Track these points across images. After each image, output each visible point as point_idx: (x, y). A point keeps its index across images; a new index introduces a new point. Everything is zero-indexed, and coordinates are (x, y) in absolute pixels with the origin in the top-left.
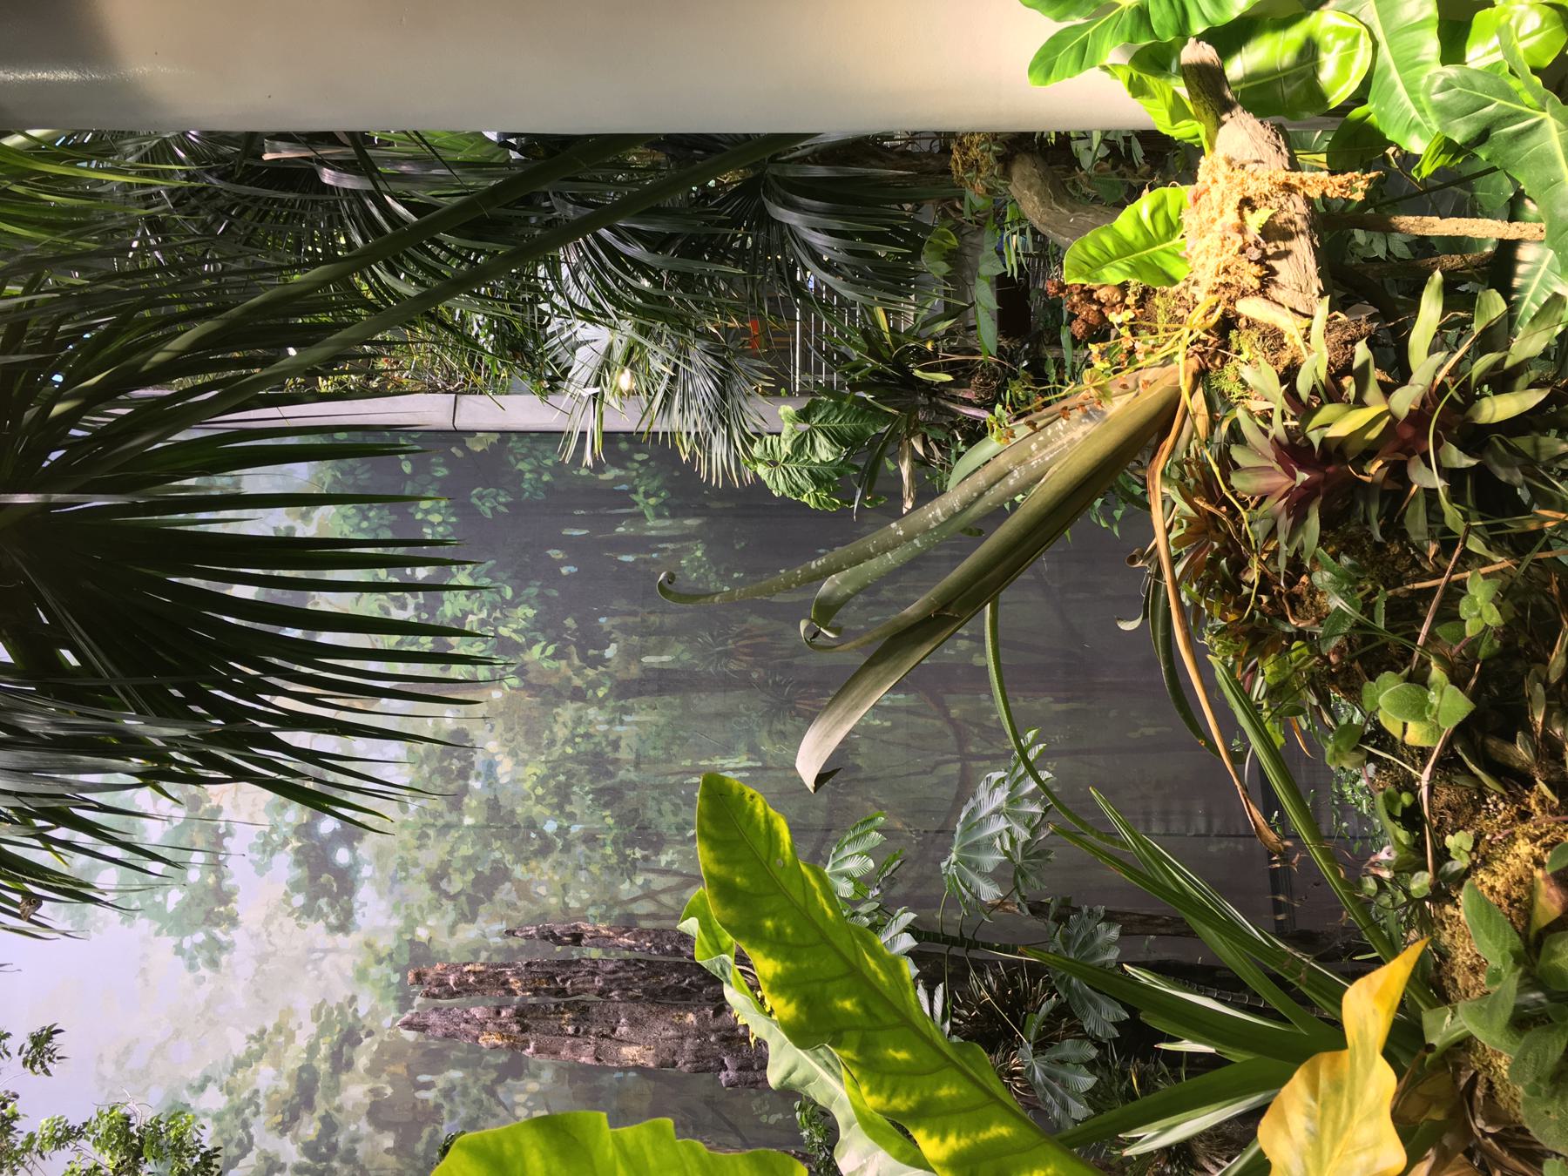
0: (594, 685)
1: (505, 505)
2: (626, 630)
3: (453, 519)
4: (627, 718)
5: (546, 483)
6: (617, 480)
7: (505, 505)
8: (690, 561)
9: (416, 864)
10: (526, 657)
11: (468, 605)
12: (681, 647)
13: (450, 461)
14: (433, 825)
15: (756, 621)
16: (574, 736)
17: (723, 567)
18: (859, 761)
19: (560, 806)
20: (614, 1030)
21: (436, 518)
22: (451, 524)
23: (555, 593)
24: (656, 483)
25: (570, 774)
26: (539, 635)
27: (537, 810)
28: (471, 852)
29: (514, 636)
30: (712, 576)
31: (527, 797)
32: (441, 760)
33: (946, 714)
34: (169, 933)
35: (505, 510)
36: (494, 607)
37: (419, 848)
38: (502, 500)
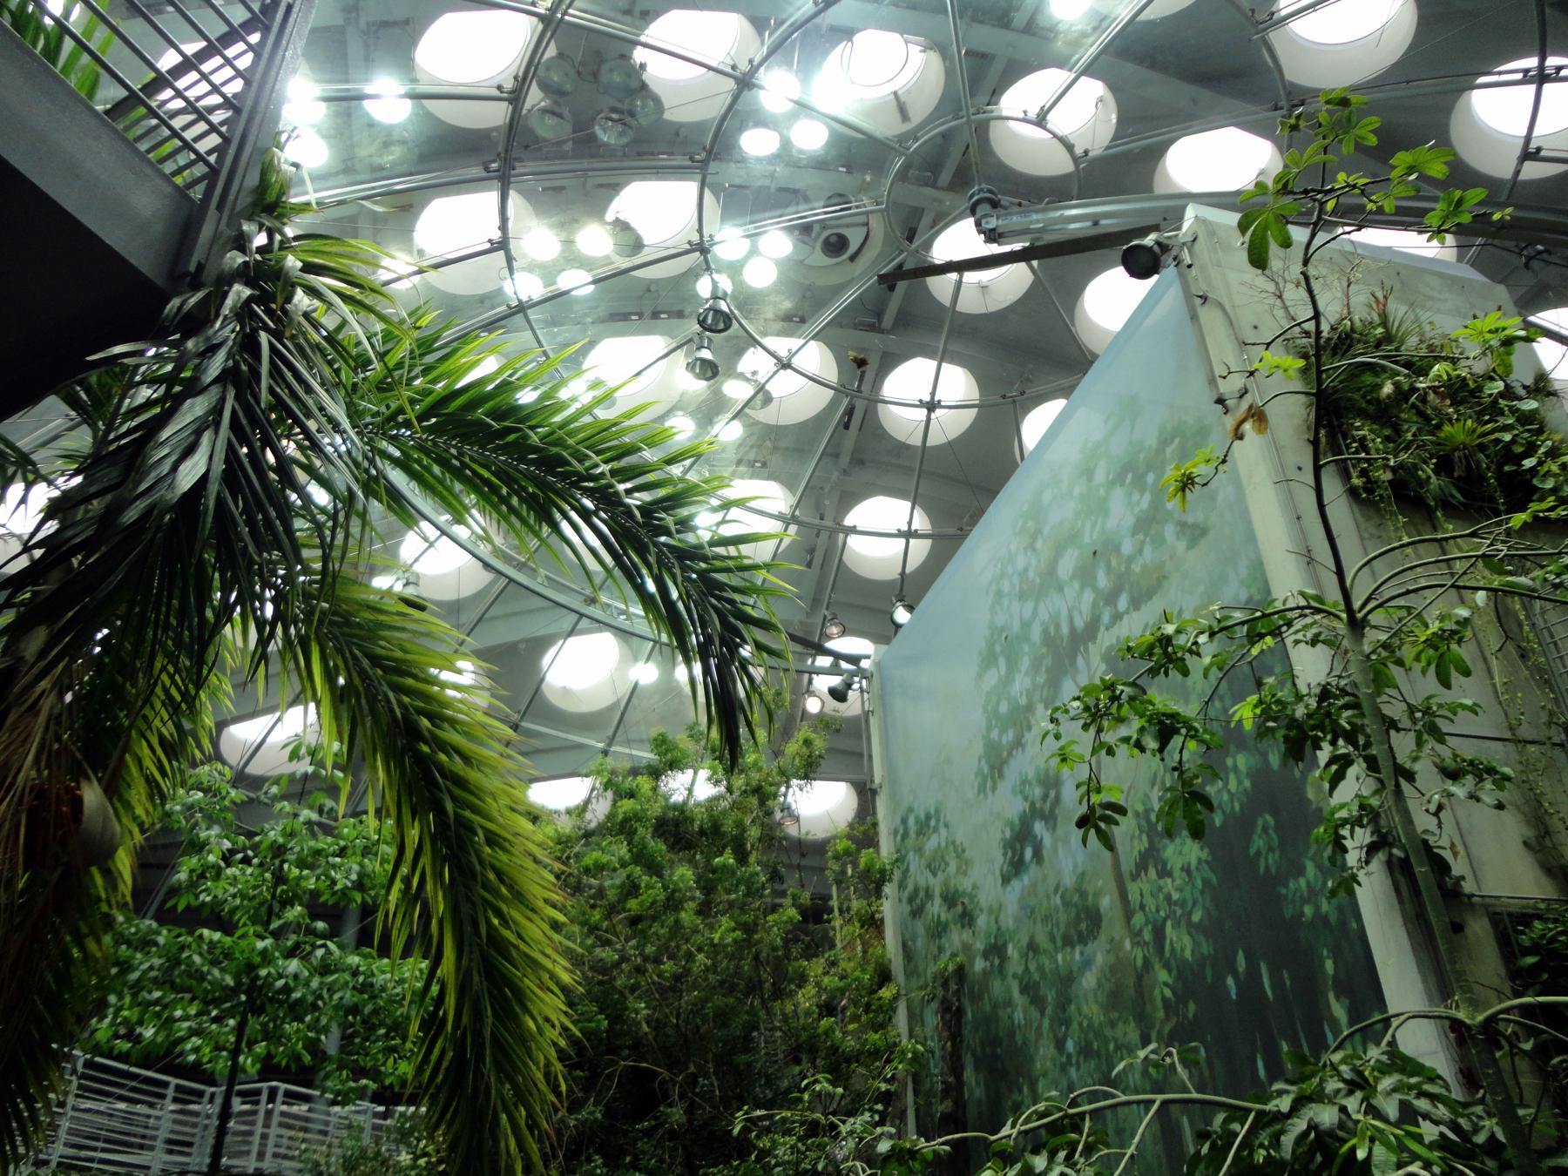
1: (1267, 867)
3: (1237, 806)
10: (1157, 966)
27: (1075, 1026)
31: (1079, 1010)
35: (1262, 870)
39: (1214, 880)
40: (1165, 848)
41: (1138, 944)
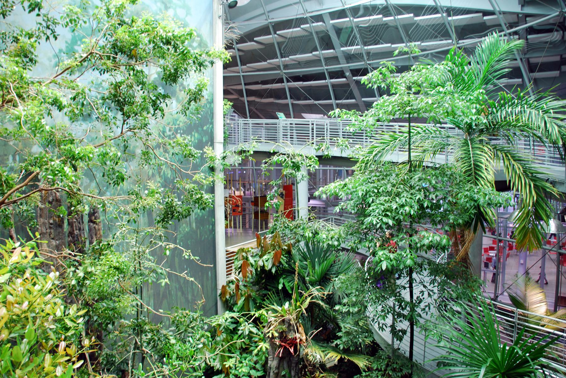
20: (53, 239)
26: (163, 180)
30: (181, 235)
34: (67, 47)
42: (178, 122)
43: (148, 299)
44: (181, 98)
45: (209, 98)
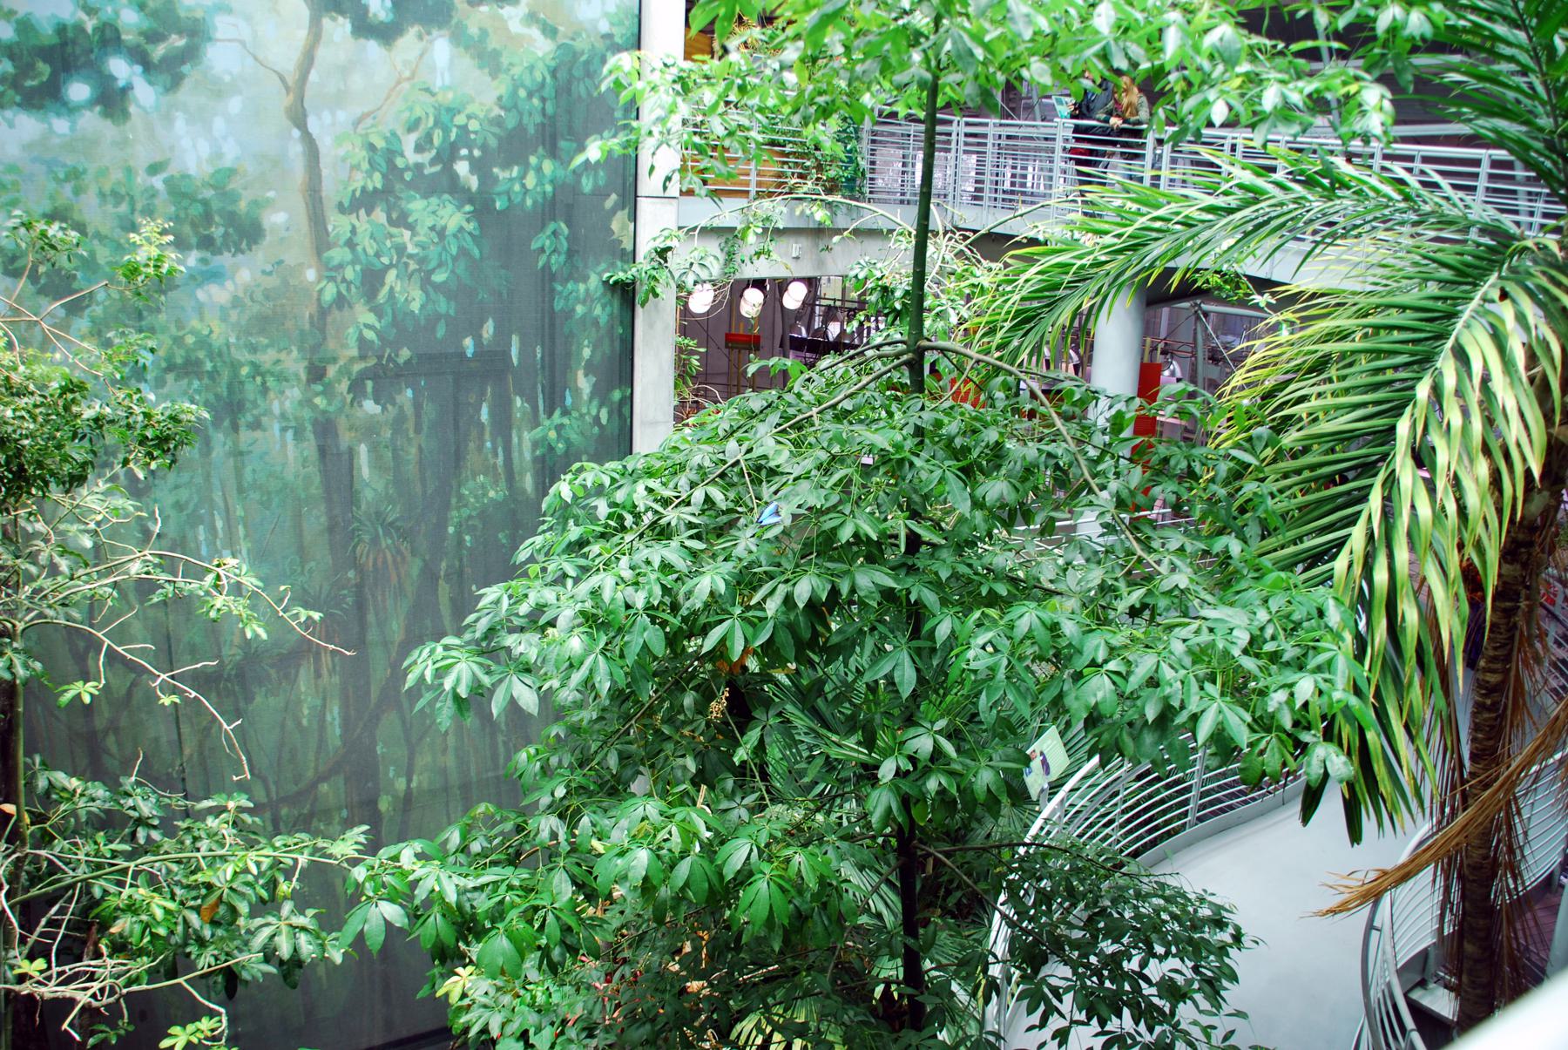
0: (328, 392)
1: (547, 266)
2: (398, 423)
3: (529, 202)
4: (290, 434)
5: (573, 310)
6: (577, 392)
7: (547, 266)
8: (483, 487)
9: (77, 191)
11: (422, 230)
12: (380, 486)
13: (600, 194)
14: (133, 211)
15: (415, 567)
16: (263, 375)
17: (476, 522)
18: (259, 699)
19: (171, 367)
21: (531, 181)
22: (524, 200)
23: (441, 331)
24: (574, 437)
25: (214, 375)
26: (388, 318)
28: (101, 261)
29: (384, 291)
30: (465, 512)
31: (180, 325)
32: (221, 212)
33: (323, 778)
35: (541, 264)
36: (422, 261)
37: (102, 195)
38: (553, 259)
39: (476, 252)
40: (410, 199)
41: (332, 279)
42: (460, 120)
43: (319, 702)
44: (473, 30)
45: (617, 31)
